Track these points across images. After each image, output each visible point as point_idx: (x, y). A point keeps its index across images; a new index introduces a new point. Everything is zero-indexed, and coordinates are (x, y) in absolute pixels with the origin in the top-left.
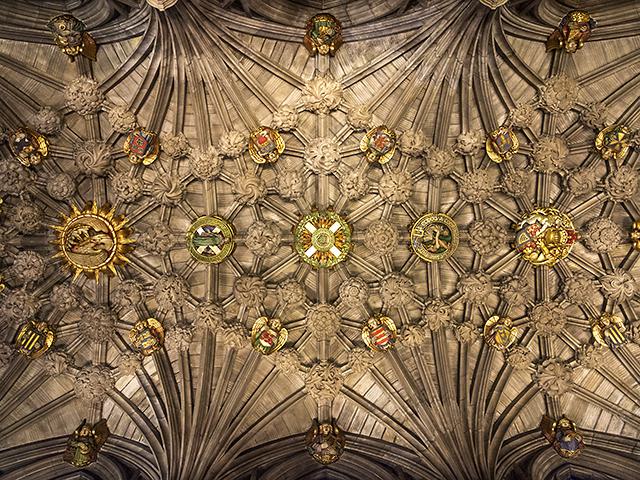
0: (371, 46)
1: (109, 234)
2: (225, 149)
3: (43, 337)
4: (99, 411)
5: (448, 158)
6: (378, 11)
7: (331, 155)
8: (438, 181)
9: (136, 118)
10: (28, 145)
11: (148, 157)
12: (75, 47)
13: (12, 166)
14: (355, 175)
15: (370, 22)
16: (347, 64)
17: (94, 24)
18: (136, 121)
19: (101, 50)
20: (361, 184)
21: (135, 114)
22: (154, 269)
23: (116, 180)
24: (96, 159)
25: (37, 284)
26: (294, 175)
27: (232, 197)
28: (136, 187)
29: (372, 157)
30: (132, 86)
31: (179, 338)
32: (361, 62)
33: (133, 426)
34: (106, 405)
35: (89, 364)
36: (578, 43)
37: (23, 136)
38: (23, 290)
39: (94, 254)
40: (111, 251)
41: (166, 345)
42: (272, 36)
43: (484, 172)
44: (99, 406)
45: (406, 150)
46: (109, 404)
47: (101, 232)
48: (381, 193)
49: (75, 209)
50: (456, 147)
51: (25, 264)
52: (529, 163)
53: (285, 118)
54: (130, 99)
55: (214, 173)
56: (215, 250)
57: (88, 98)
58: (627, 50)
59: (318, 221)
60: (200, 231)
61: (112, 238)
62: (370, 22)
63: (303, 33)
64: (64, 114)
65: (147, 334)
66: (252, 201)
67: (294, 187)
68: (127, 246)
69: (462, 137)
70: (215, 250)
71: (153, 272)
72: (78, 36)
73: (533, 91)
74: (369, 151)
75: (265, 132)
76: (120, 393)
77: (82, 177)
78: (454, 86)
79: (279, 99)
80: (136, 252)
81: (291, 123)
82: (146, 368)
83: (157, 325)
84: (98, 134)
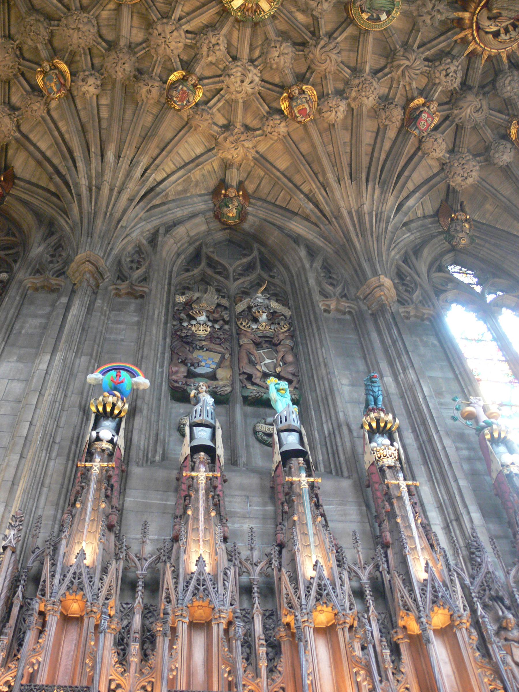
0: (185, 191)
5: (113, 72)
6: (181, 230)
7: (234, 81)
8: (122, 43)
12: (457, 219)
14: (210, 59)
16: (209, 172)
17: (436, 240)
19: (435, 210)
20: (205, 49)
24: (471, 109)
26: (274, 66)
28: (437, 75)
29: (192, 80)
30: (419, 175)
32: (196, 174)
42: (281, 211)
43: (70, 48)
45: (156, 84)
48: (183, 35)
50: (102, 80)
52: (20, 49)
53: (276, 130)
54: (423, 163)
55: (357, 81)
57: (459, 170)
59: (255, 11)
60: (384, 17)
63: (250, 209)
64: (484, 154)
66: (322, 43)
67: (277, 54)
69: (97, 92)
72: (452, 229)
73: (24, 129)
74: (195, 86)
75: (299, 119)
77: (487, 89)
78: (110, 156)
79: (279, 146)
81: (271, 123)
84: (459, 130)
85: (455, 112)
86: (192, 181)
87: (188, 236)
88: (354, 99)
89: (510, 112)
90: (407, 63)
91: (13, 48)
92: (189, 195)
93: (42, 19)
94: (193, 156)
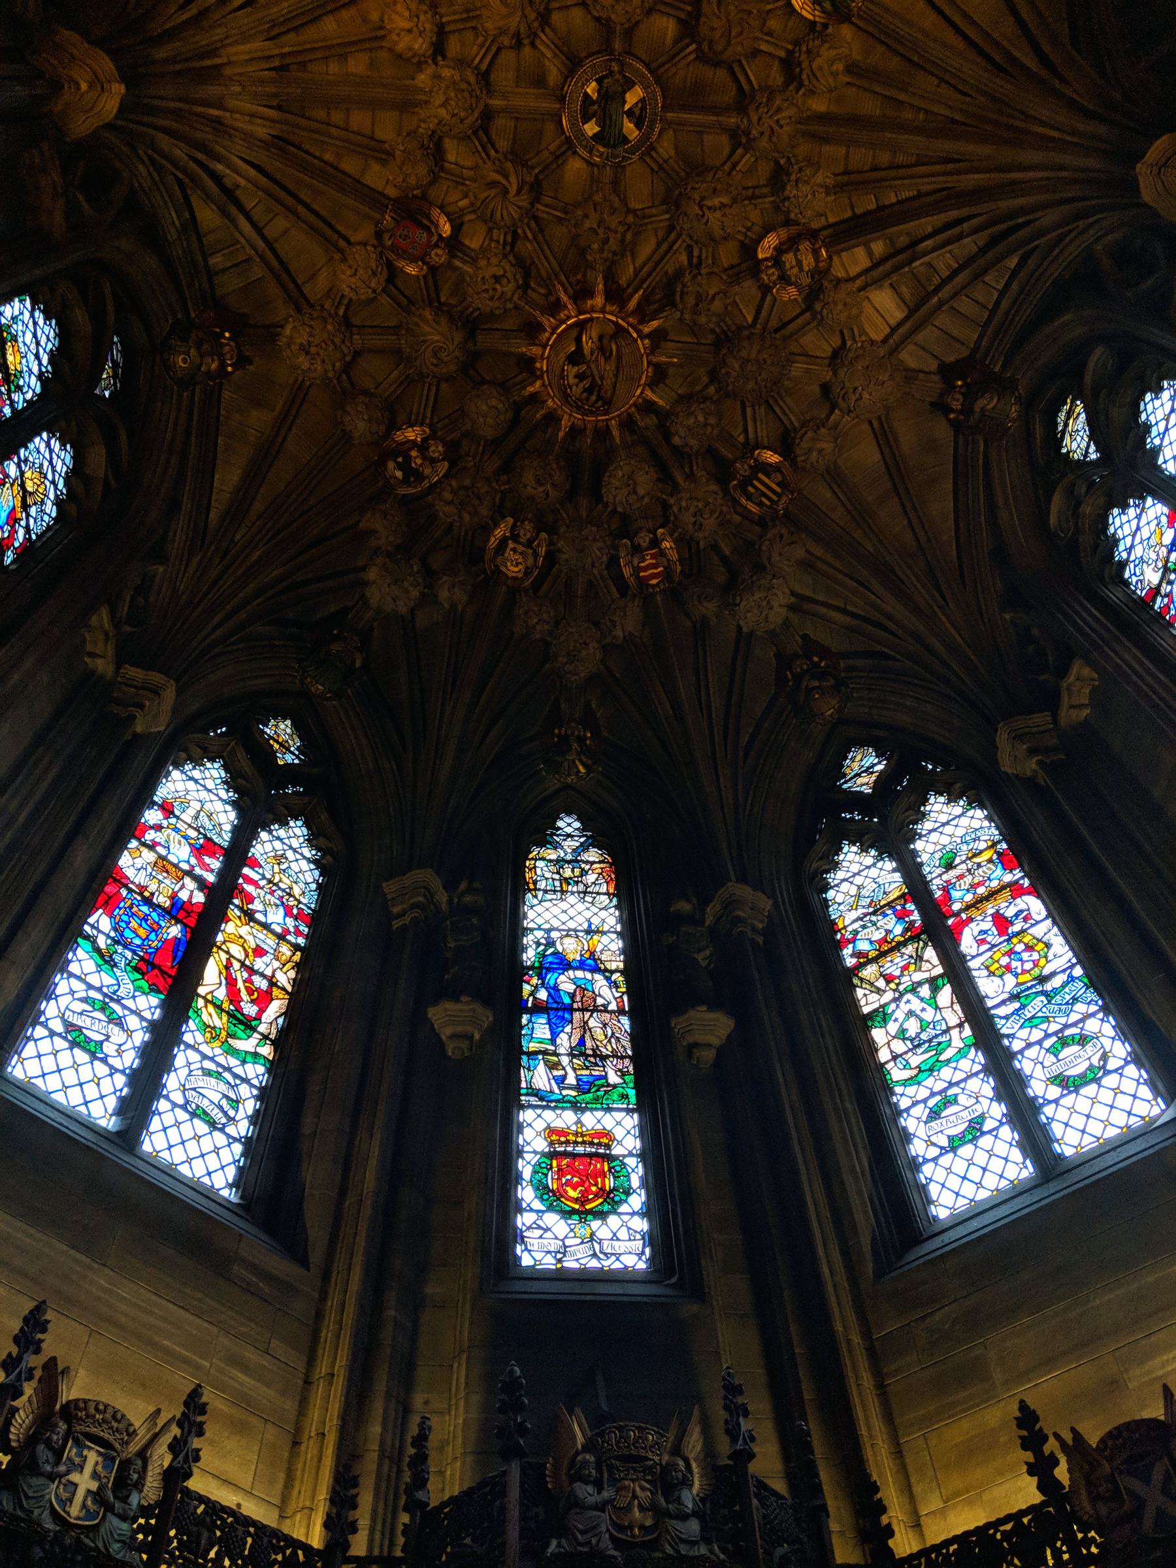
1: (581, 326)
2: (421, 45)
3: (767, 468)
4: (922, 375)
9: (359, 243)
10: (408, 459)
11: (437, 226)
13: (448, 496)
18: (365, 245)
21: (349, 243)
22: (659, 245)
23: (481, 302)
25: (665, 476)
27: (527, 51)
31: (805, 189)
33: (964, 305)
34: (912, 363)
35: (826, 388)
37: (391, 465)
38: (672, 501)
39: (619, 357)
40: (616, 324)
41: (815, 225)
44: (910, 375)
46: (909, 357)
47: (578, 340)
49: (531, 389)
51: (625, 491)
55: (472, 79)
56: (632, 98)
60: (591, 128)
61: (591, 319)
65: (789, 258)
68: (610, 296)
70: (632, 98)
71: (665, 246)
76: (893, 330)
80: (623, 282)
82: (854, 271)
83: (771, 241)
85: (428, 314)
88: (437, 77)
89: (439, 425)
90: (513, 189)
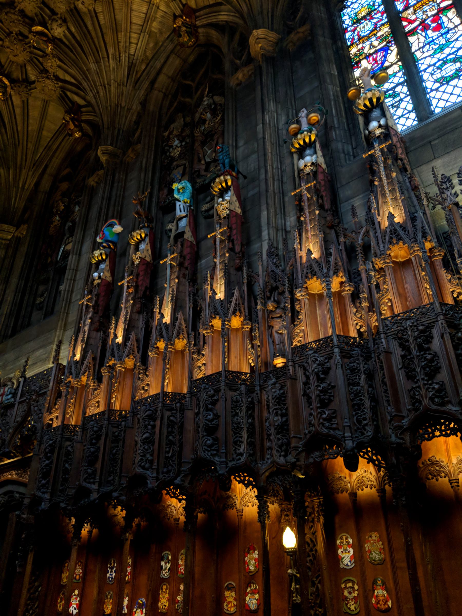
0: (156, 44)
15: (165, 62)
16: (162, 17)
36: (66, 121)
58: (45, 133)
62: (165, 62)
63: (198, 23)
86: (156, 33)
87: (169, 77)
91: (15, 39)
92: (161, 44)
93: (8, 10)
94: (143, 15)
